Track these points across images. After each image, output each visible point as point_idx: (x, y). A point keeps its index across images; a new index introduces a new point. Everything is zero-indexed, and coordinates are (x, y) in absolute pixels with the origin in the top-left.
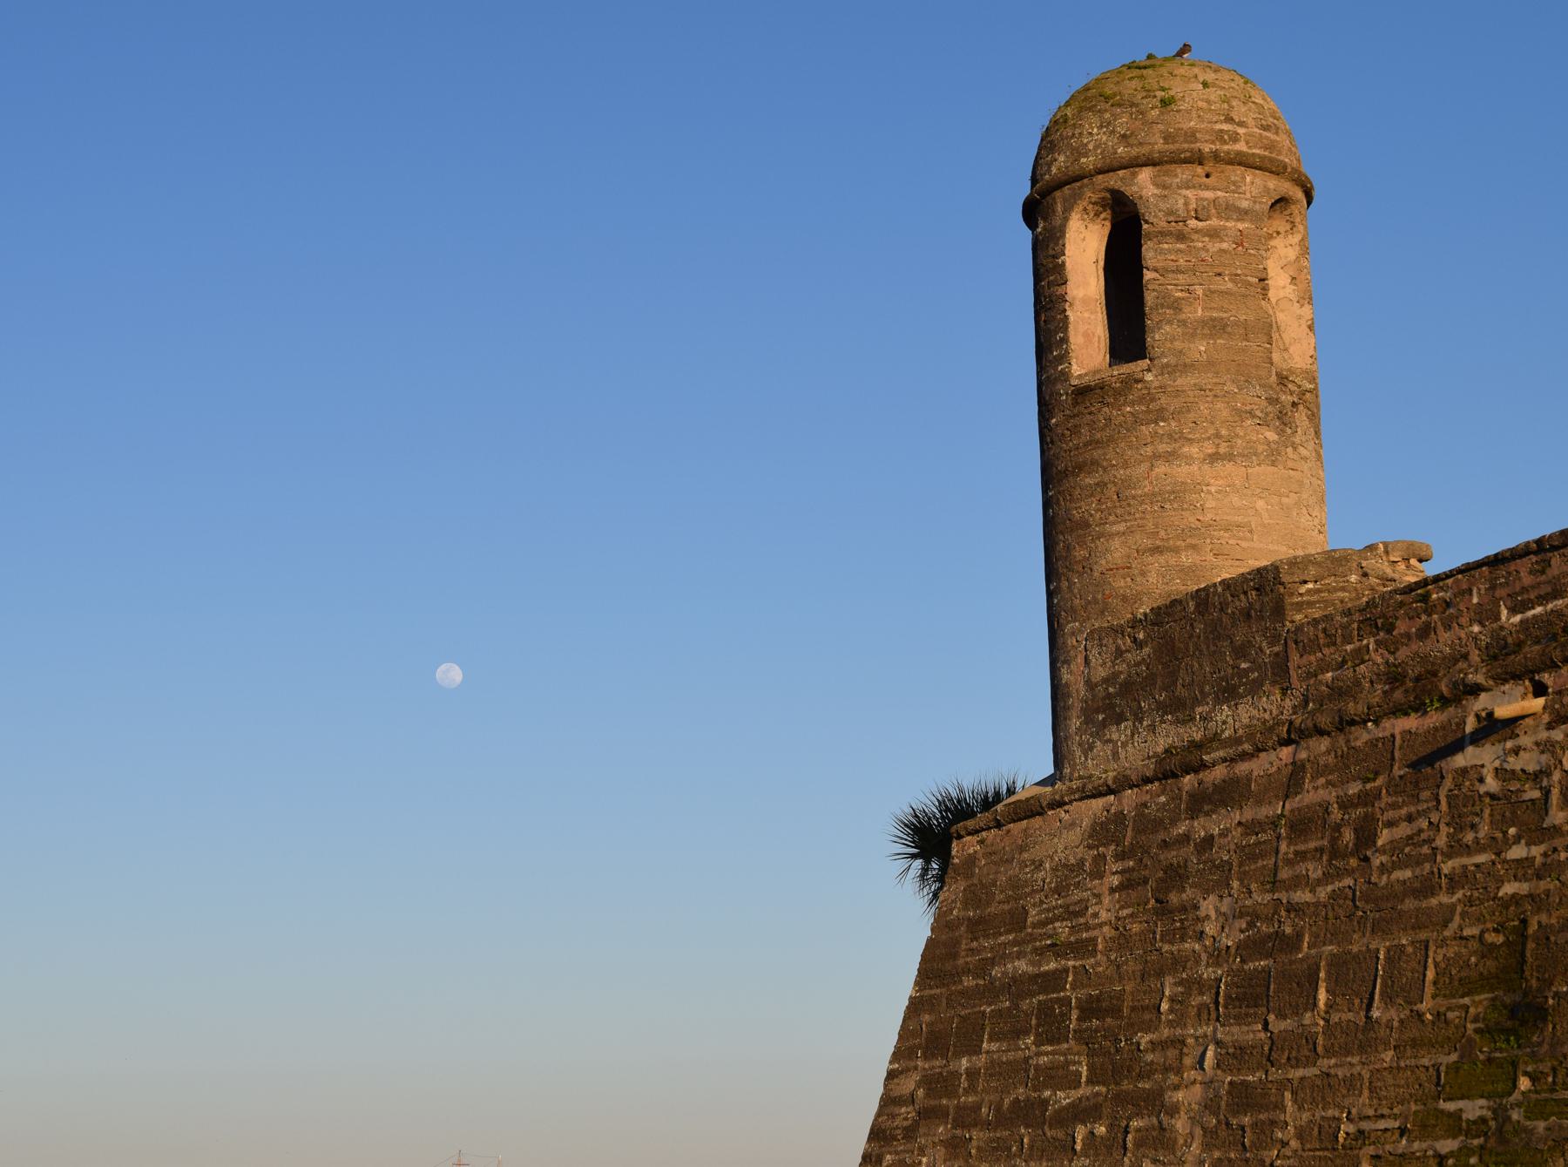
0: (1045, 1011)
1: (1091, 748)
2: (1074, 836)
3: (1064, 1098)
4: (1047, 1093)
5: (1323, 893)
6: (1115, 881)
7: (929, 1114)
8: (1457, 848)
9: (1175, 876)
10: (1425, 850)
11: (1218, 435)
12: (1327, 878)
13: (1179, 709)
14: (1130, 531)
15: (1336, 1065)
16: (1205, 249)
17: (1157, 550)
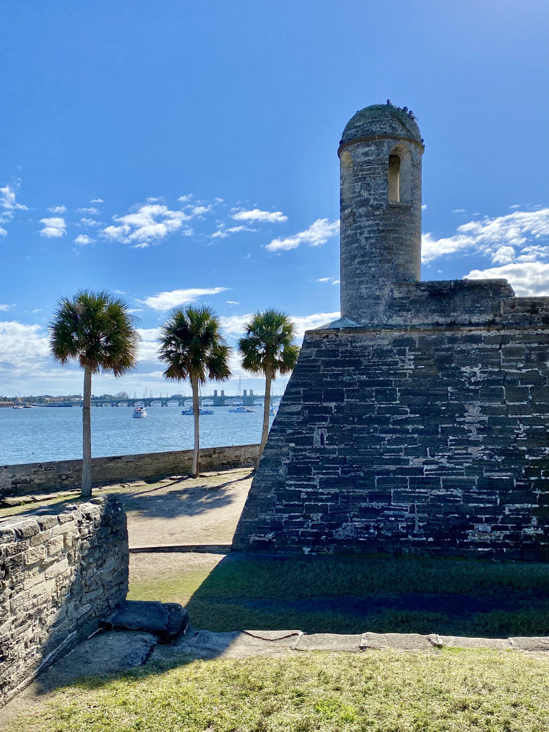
0: (378, 392)
1: (391, 317)
2: (386, 342)
4: (388, 415)
5: (524, 371)
6: (412, 357)
9: (449, 359)
12: (523, 368)
13: (442, 312)
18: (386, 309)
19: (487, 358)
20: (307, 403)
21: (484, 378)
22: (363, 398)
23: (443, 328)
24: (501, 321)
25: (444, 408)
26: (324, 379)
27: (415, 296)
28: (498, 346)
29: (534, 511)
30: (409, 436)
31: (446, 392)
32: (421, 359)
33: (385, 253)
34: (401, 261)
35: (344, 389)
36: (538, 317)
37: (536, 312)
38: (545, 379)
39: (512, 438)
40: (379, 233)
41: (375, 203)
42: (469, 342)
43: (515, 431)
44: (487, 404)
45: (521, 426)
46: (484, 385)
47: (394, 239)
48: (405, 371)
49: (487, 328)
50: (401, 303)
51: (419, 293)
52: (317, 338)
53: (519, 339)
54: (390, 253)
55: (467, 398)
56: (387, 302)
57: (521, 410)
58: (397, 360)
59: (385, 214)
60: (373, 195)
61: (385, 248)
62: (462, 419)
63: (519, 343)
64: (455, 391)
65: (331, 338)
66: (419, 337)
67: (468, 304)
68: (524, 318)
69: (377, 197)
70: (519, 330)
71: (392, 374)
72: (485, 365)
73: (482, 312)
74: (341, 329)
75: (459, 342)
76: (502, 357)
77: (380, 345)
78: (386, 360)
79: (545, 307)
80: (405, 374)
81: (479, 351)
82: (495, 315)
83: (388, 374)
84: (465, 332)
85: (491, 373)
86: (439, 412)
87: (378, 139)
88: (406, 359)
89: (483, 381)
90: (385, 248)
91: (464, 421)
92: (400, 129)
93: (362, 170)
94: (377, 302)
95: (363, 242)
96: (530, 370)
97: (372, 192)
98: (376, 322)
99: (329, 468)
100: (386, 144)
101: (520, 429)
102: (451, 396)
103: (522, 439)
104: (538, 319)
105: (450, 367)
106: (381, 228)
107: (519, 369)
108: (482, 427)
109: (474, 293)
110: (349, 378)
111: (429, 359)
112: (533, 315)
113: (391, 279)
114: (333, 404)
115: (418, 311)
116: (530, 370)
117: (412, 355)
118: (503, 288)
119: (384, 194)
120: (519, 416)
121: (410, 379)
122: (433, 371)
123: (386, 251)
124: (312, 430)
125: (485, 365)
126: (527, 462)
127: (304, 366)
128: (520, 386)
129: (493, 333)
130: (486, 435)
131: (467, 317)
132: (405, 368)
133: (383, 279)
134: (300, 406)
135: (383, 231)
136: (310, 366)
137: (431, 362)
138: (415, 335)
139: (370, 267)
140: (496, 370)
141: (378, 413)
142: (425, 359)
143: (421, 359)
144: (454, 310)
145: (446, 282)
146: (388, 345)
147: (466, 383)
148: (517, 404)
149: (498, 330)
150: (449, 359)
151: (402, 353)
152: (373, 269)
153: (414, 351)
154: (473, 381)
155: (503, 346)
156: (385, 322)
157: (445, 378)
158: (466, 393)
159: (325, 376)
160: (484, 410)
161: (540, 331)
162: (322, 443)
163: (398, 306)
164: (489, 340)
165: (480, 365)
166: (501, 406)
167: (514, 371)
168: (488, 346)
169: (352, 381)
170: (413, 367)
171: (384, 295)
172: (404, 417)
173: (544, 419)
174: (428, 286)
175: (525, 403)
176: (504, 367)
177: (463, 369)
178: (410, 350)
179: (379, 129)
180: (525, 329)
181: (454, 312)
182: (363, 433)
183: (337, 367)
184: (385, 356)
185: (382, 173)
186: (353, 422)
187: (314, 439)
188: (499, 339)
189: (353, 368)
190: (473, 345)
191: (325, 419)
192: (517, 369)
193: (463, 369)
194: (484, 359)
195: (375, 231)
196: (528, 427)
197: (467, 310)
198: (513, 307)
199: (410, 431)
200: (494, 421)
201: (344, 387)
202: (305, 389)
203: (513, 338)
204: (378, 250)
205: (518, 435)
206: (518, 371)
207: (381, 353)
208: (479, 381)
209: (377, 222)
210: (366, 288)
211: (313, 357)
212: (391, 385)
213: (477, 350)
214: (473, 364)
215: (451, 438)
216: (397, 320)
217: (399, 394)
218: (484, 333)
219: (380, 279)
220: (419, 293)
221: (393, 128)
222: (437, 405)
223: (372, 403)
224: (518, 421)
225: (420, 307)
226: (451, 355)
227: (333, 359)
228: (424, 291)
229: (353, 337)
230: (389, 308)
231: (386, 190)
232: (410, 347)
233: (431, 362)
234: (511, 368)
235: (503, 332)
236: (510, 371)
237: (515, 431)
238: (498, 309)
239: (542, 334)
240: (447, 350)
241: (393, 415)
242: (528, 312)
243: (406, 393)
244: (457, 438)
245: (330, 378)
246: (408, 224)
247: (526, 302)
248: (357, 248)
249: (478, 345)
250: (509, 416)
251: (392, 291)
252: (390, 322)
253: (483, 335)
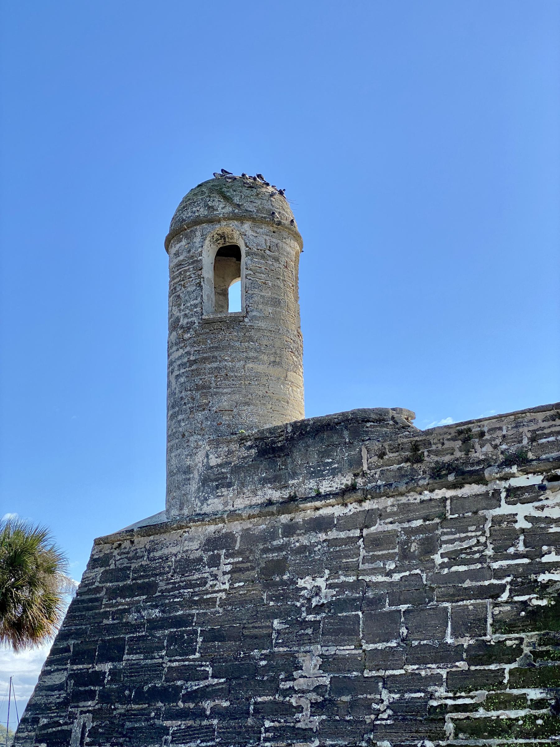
0: (172, 639)
1: (206, 499)
2: (195, 545)
3: (194, 686)
4: (179, 683)
5: (397, 577)
6: (229, 568)
7: (78, 697)
8: (500, 553)
9: (279, 567)
10: (477, 556)
11: (275, 353)
13: (277, 481)
14: (233, 393)
15: (418, 669)
16: (273, 265)
17: (247, 404)
18: (199, 488)
19: (341, 557)
20: (75, 667)
21: (333, 596)
22: (148, 652)
23: (274, 508)
24: (365, 484)
25: (263, 663)
26: (105, 622)
27: (239, 458)
28: (357, 533)
30: (205, 723)
31: (270, 630)
32: (240, 570)
33: (198, 395)
34: (225, 405)
35: (127, 636)
36: (423, 467)
37: (419, 460)
38: (432, 589)
39: (368, 721)
40: (190, 366)
41: (186, 321)
42: (314, 530)
43: (374, 706)
44: (332, 650)
45: (385, 694)
46: (329, 611)
47: (212, 371)
48: (214, 595)
49: (340, 499)
50: (219, 474)
51: (244, 453)
52: (107, 548)
53: (392, 514)
54: (205, 395)
55: (301, 641)
56: (200, 475)
57: (385, 658)
58: (205, 575)
59: (198, 335)
60: (183, 311)
61: (198, 388)
62: (288, 684)
63: (391, 523)
64: (284, 626)
65: (125, 548)
66: (243, 530)
67: (314, 459)
68: (401, 475)
69: (187, 311)
70: (392, 496)
71: (196, 603)
72: (334, 573)
73: (334, 473)
74: (135, 530)
75: (298, 532)
76: (363, 552)
77: (187, 551)
78: (190, 578)
79: (434, 447)
80: (213, 601)
81: (328, 546)
82: (356, 475)
83: (191, 603)
84: (307, 512)
85: (343, 586)
86: (257, 670)
87: (188, 228)
88: (220, 573)
89: (330, 603)
90: (198, 388)
91: (292, 688)
92: (221, 206)
94: (188, 477)
96: (407, 573)
97: (182, 307)
98: (186, 511)
100: (198, 234)
101: (382, 701)
102: (277, 639)
103: (384, 722)
104: (424, 472)
105: (281, 580)
106: (192, 358)
107: (389, 574)
108: (320, 699)
109: (322, 440)
110: (136, 615)
111: (253, 568)
112: (415, 466)
113: (207, 436)
114: (107, 667)
115: (243, 485)
116: (407, 573)
117: (229, 564)
118: (368, 424)
119: (195, 306)
120: (381, 673)
121: (221, 610)
122: (256, 591)
123: (200, 392)
124: (72, 716)
125: (334, 573)
127: (83, 601)
128: (387, 608)
129: (352, 508)
130: (324, 717)
131: (312, 484)
132: (216, 589)
133: (196, 437)
134: (65, 673)
135: (195, 361)
136: (91, 600)
137: (255, 574)
138: (236, 527)
139: (179, 422)
140: (351, 579)
141: (167, 680)
142: (247, 569)
143: (240, 570)
144: (294, 475)
145: (279, 427)
146: (197, 550)
147: (304, 609)
148: (380, 646)
149: (360, 502)
150: (279, 567)
151: (214, 562)
152: (183, 424)
154: (314, 605)
155: (365, 532)
156: (198, 512)
157: (272, 603)
158: (301, 631)
159: (106, 615)
160: (327, 664)
161: (427, 495)
163: (217, 481)
164: (346, 523)
165: (327, 572)
166: (354, 652)
167: (381, 578)
168: (342, 535)
169: (139, 621)
170: (227, 586)
171: (196, 465)
172: (202, 684)
173: (426, 677)
174: (256, 439)
175: (393, 644)
177: (301, 583)
178: (227, 556)
179: (190, 214)
180: (402, 494)
181: (293, 479)
182: (140, 721)
183: (124, 598)
184: (191, 571)
185: (193, 276)
186: (128, 700)
187: (73, 734)
188: (361, 519)
189: (145, 597)
190: (320, 535)
191: (91, 695)
192: (384, 574)
193: (301, 583)
194: (336, 559)
195: (185, 364)
196: (397, 696)
197: (313, 472)
198: (381, 456)
199: (208, 713)
200: (339, 685)
201: (127, 634)
202: (76, 642)
203: (381, 514)
204: (189, 392)
205: (378, 712)
206: (387, 579)
207: (187, 565)
208: (323, 604)
209: (188, 349)
211: (97, 584)
212: (190, 625)
213: (325, 544)
214: (316, 573)
215: (268, 724)
216: (214, 505)
217: (200, 639)
218: (338, 511)
219: (192, 439)
220: (244, 453)
221: (209, 207)
222: (254, 658)
223: (160, 661)
224: (380, 684)
225: (245, 477)
226: (285, 558)
227: (121, 584)
228: (251, 447)
229: (153, 541)
230: (203, 485)
231: (199, 299)
232: (228, 550)
233: (255, 574)
234: (374, 574)
235: (367, 505)
236: (374, 579)
237: (374, 706)
238: (357, 462)
239: (431, 500)
240: (280, 549)
241: (187, 681)
242: (406, 462)
244: (277, 724)
245: (113, 619)
246: (238, 344)
247: (402, 443)
249: (326, 535)
251: (207, 456)
252: (206, 509)
253: (336, 515)
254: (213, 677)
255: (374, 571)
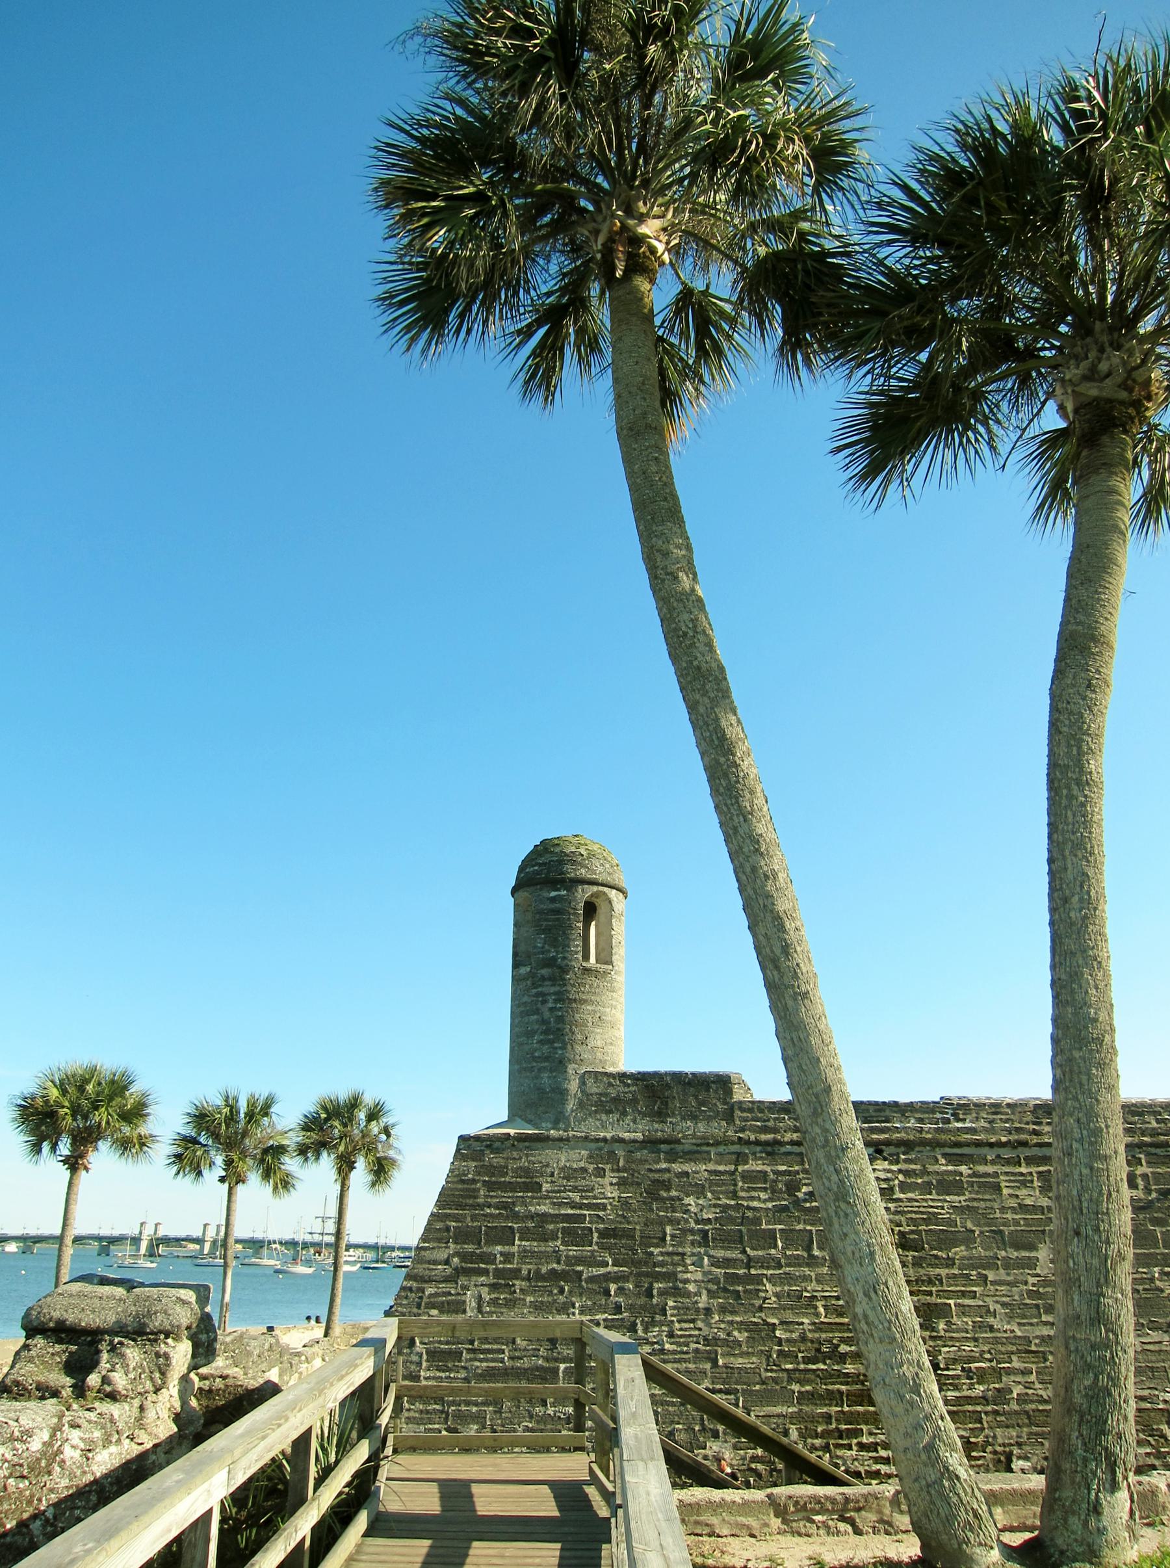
5: (770, 1205)
6: (614, 1181)
29: (792, 1418)
80: (603, 1207)
93: (546, 920)
95: (547, 1015)
99: (489, 1351)
124: (465, 1288)
126: (780, 1342)
144: (674, 1115)
153: (618, 1171)
162: (480, 1311)
172: (602, 1270)
176: (743, 1198)
178: (613, 1170)
191: (485, 1272)
210: (549, 1077)
243: (603, 1234)
248: (537, 1021)
250: (753, 1272)
254: (613, 1265)
255: (752, 1198)
